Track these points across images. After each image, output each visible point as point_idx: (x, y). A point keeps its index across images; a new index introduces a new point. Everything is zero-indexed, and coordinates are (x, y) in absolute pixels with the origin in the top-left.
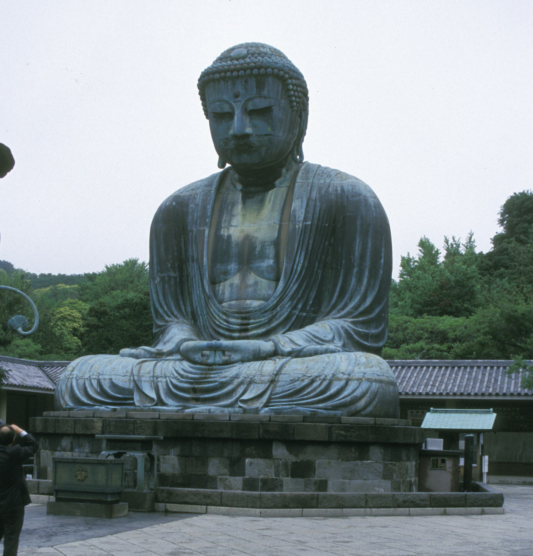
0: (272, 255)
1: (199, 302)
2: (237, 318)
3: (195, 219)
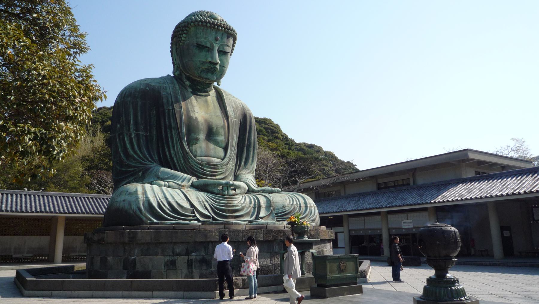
0: (223, 134)
1: (175, 155)
2: (209, 168)
3: (170, 102)
